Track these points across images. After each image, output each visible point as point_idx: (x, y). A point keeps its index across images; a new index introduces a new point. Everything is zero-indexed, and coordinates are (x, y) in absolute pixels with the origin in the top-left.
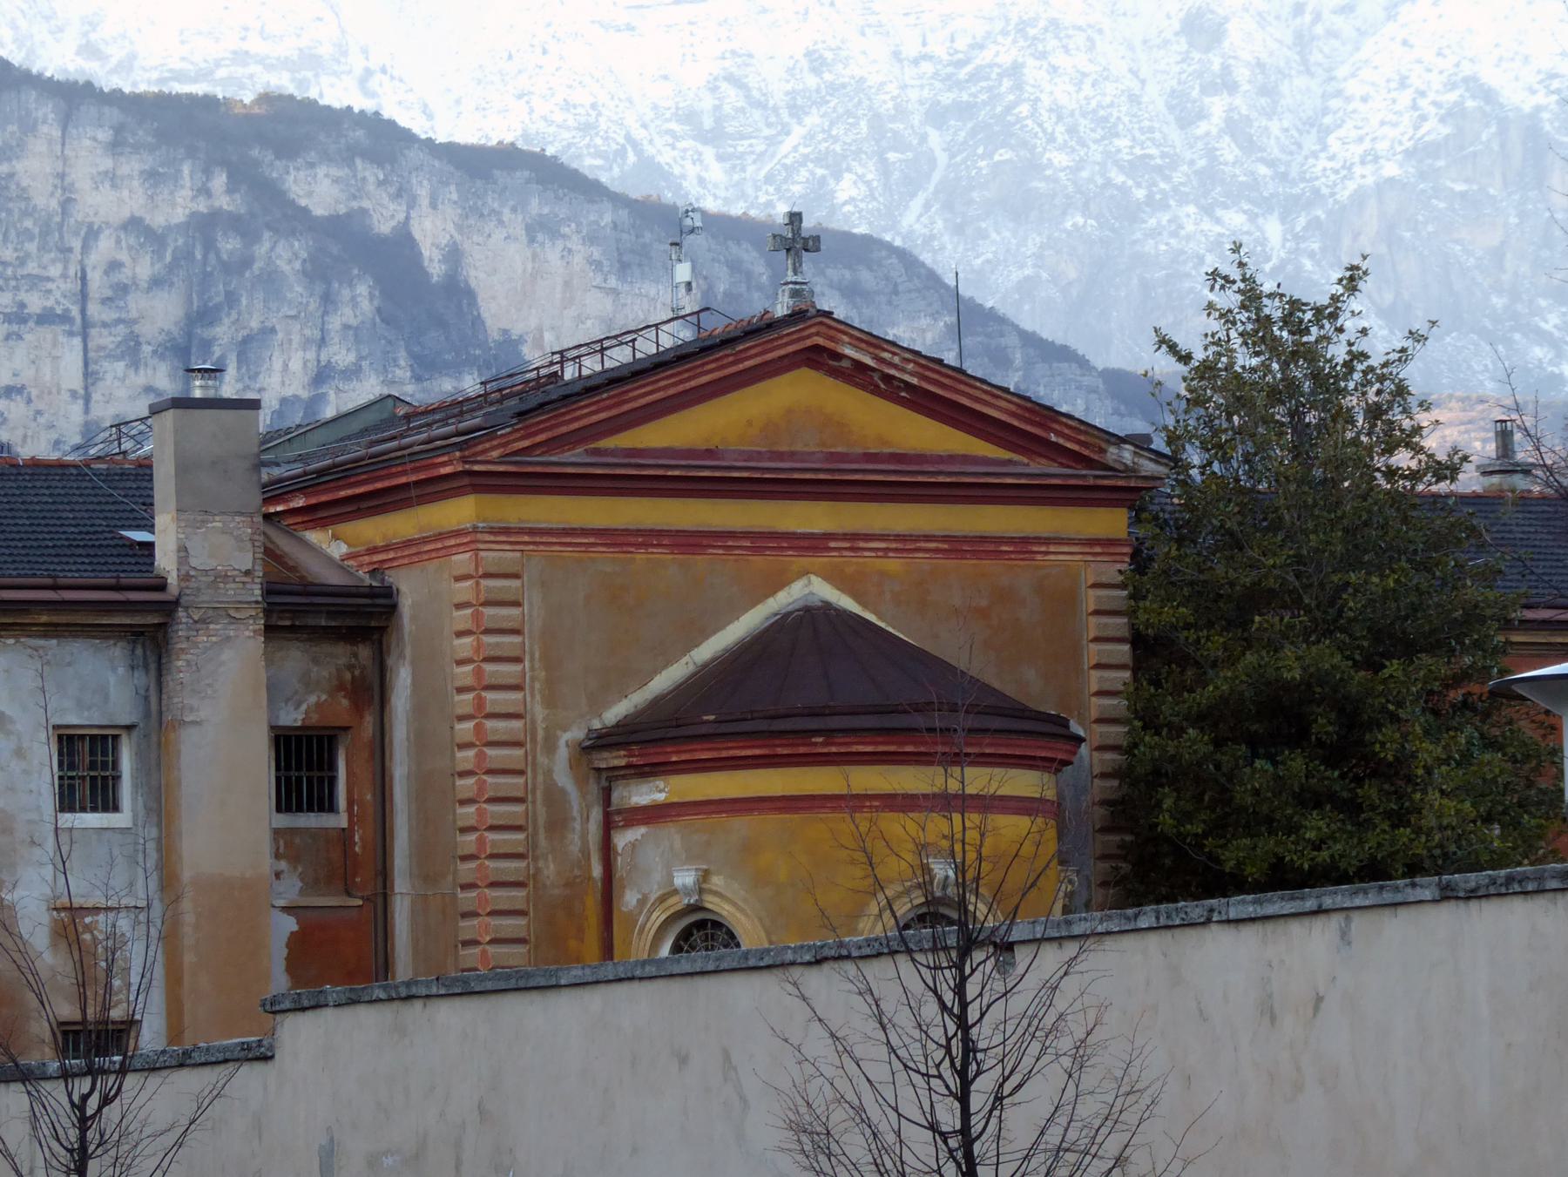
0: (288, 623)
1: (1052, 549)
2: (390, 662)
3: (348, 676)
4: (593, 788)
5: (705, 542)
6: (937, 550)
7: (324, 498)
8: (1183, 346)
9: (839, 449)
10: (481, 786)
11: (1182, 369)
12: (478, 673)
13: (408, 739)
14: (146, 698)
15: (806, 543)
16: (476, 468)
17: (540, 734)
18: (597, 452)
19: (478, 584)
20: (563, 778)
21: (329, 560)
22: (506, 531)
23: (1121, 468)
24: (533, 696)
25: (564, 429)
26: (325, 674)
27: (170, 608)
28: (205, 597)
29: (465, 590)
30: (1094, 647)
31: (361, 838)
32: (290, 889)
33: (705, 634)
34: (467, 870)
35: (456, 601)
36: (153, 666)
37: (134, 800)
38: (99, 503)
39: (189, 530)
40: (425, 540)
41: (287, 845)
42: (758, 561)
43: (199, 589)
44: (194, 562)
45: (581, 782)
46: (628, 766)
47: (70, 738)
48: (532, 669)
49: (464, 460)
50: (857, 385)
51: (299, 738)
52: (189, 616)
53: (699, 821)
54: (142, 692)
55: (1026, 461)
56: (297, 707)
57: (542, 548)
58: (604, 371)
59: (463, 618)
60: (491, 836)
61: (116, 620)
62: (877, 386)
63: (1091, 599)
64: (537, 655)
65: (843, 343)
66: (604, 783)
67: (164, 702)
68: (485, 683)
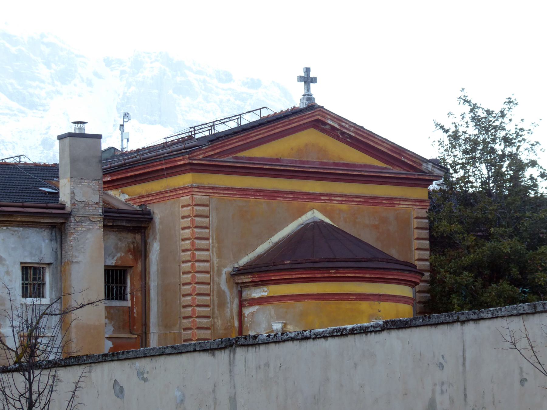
0: (111, 224)
1: (401, 203)
2: (149, 241)
3: (132, 246)
4: (235, 291)
5: (276, 195)
6: (359, 202)
7: (120, 176)
8: (446, 128)
9: (325, 161)
10: (194, 289)
11: (446, 135)
12: (193, 244)
13: (158, 271)
14: (56, 252)
15: (313, 197)
16: (194, 162)
17: (216, 269)
18: (236, 158)
19: (193, 208)
20: (224, 287)
21: (120, 201)
22: (204, 188)
23: (427, 172)
24: (213, 253)
25: (226, 148)
26: (124, 245)
27: (67, 216)
28: (81, 212)
29: (187, 211)
30: (416, 241)
31: (137, 311)
32: (109, 331)
33: (276, 231)
34: (187, 323)
35: (183, 215)
36: (59, 240)
37: (51, 293)
38: (26, 178)
39: (74, 185)
40: (166, 192)
41: (110, 313)
42: (295, 203)
43: (79, 209)
44: (77, 198)
45: (230, 288)
46: (252, 282)
47: (26, 268)
48: (213, 243)
49: (189, 159)
50: (331, 136)
51: (112, 271)
52: (75, 220)
53: (282, 304)
54: (55, 250)
55: (391, 168)
56: (113, 258)
57: (216, 195)
58: (214, 134)
59: (186, 222)
60: (198, 309)
61: (46, 221)
62: (339, 136)
63: (415, 223)
64: (215, 237)
65: (328, 119)
66: (239, 289)
67: (63, 254)
68: (196, 247)
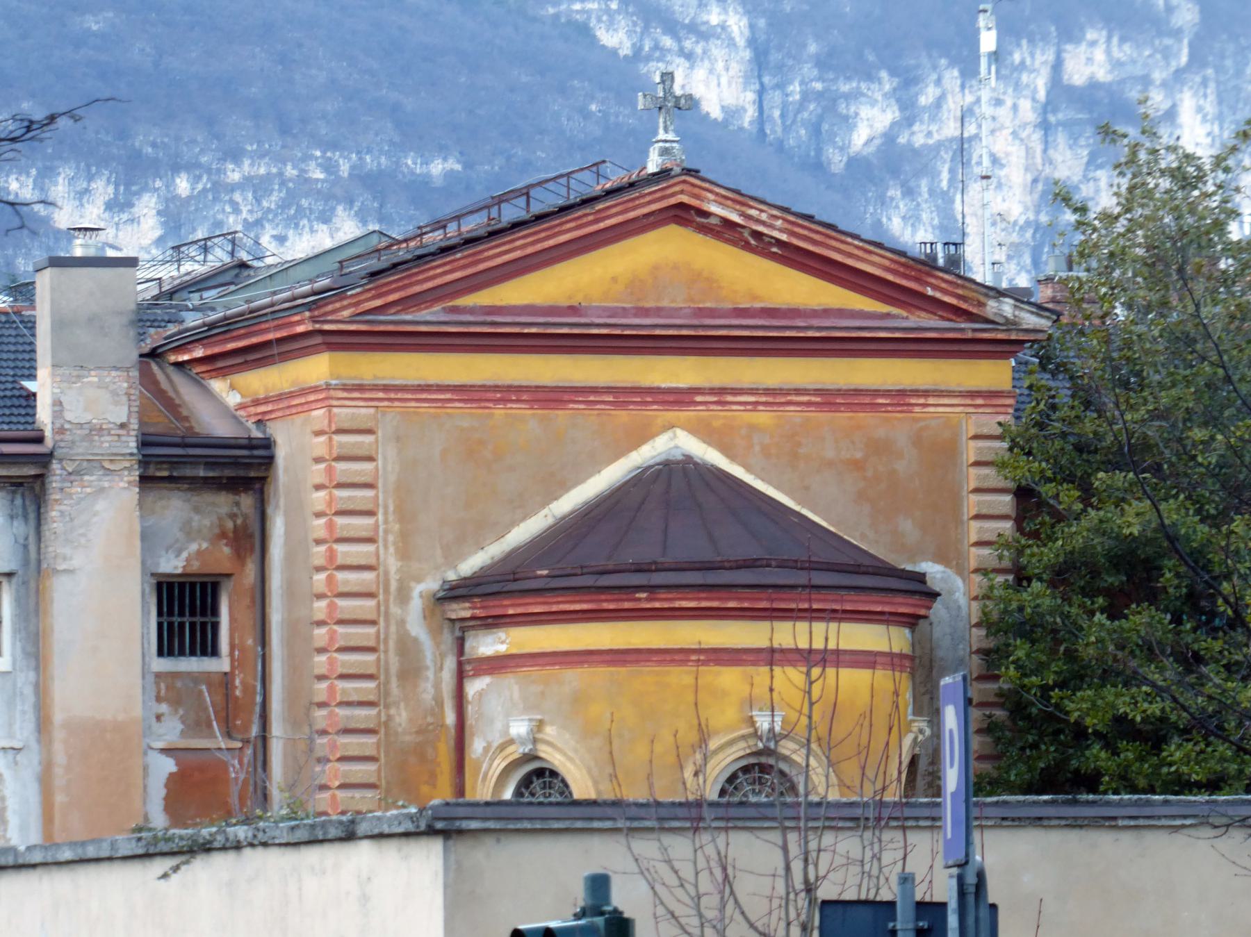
0: (165, 474)
3: (230, 525)
4: (448, 638)
5: (566, 397)
6: (809, 404)
9: (708, 305)
14: (25, 547)
15: (671, 398)
16: (327, 327)
17: (394, 585)
18: (455, 310)
19: (330, 439)
20: (417, 627)
22: (360, 388)
23: (1001, 321)
24: (386, 547)
25: (417, 289)
26: (207, 522)
27: (45, 460)
28: (81, 449)
30: (974, 498)
31: (242, 682)
32: (171, 731)
33: (564, 487)
36: (32, 516)
37: (13, 644)
39: (65, 385)
40: (291, 395)
41: (169, 691)
42: (622, 416)
43: (73, 442)
44: (69, 416)
45: (435, 632)
46: (473, 618)
48: (386, 522)
49: (314, 320)
50: (727, 241)
51: (182, 585)
52: (63, 468)
53: (535, 672)
54: (21, 541)
55: (905, 314)
56: (178, 556)
57: (397, 404)
62: (747, 243)
63: (971, 451)
64: (391, 508)
65: (709, 201)
66: (458, 633)
67: (42, 551)
